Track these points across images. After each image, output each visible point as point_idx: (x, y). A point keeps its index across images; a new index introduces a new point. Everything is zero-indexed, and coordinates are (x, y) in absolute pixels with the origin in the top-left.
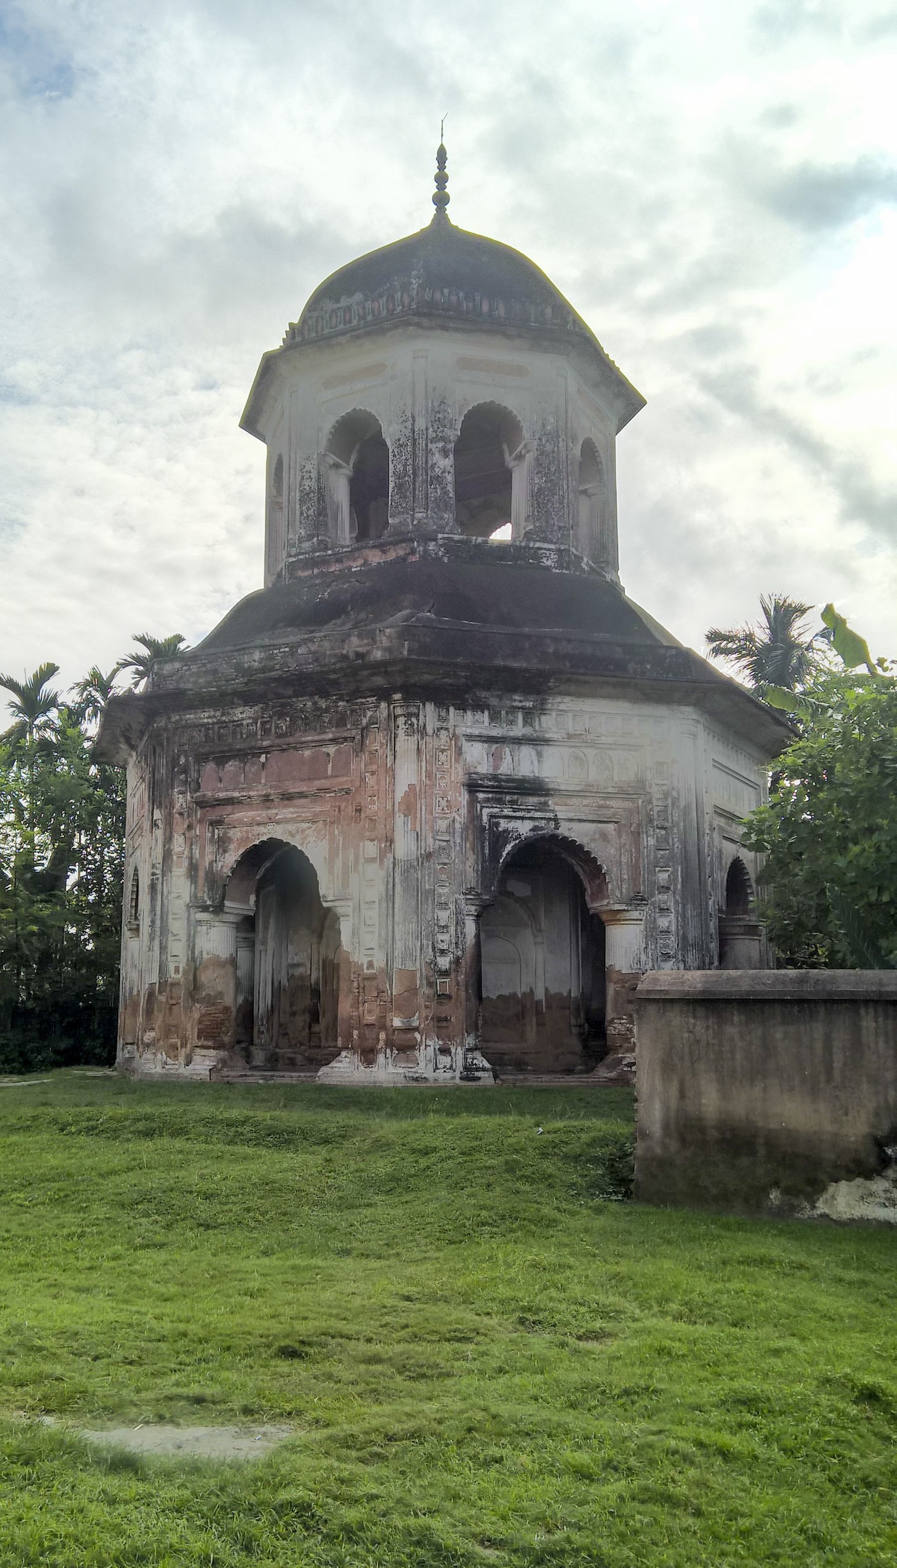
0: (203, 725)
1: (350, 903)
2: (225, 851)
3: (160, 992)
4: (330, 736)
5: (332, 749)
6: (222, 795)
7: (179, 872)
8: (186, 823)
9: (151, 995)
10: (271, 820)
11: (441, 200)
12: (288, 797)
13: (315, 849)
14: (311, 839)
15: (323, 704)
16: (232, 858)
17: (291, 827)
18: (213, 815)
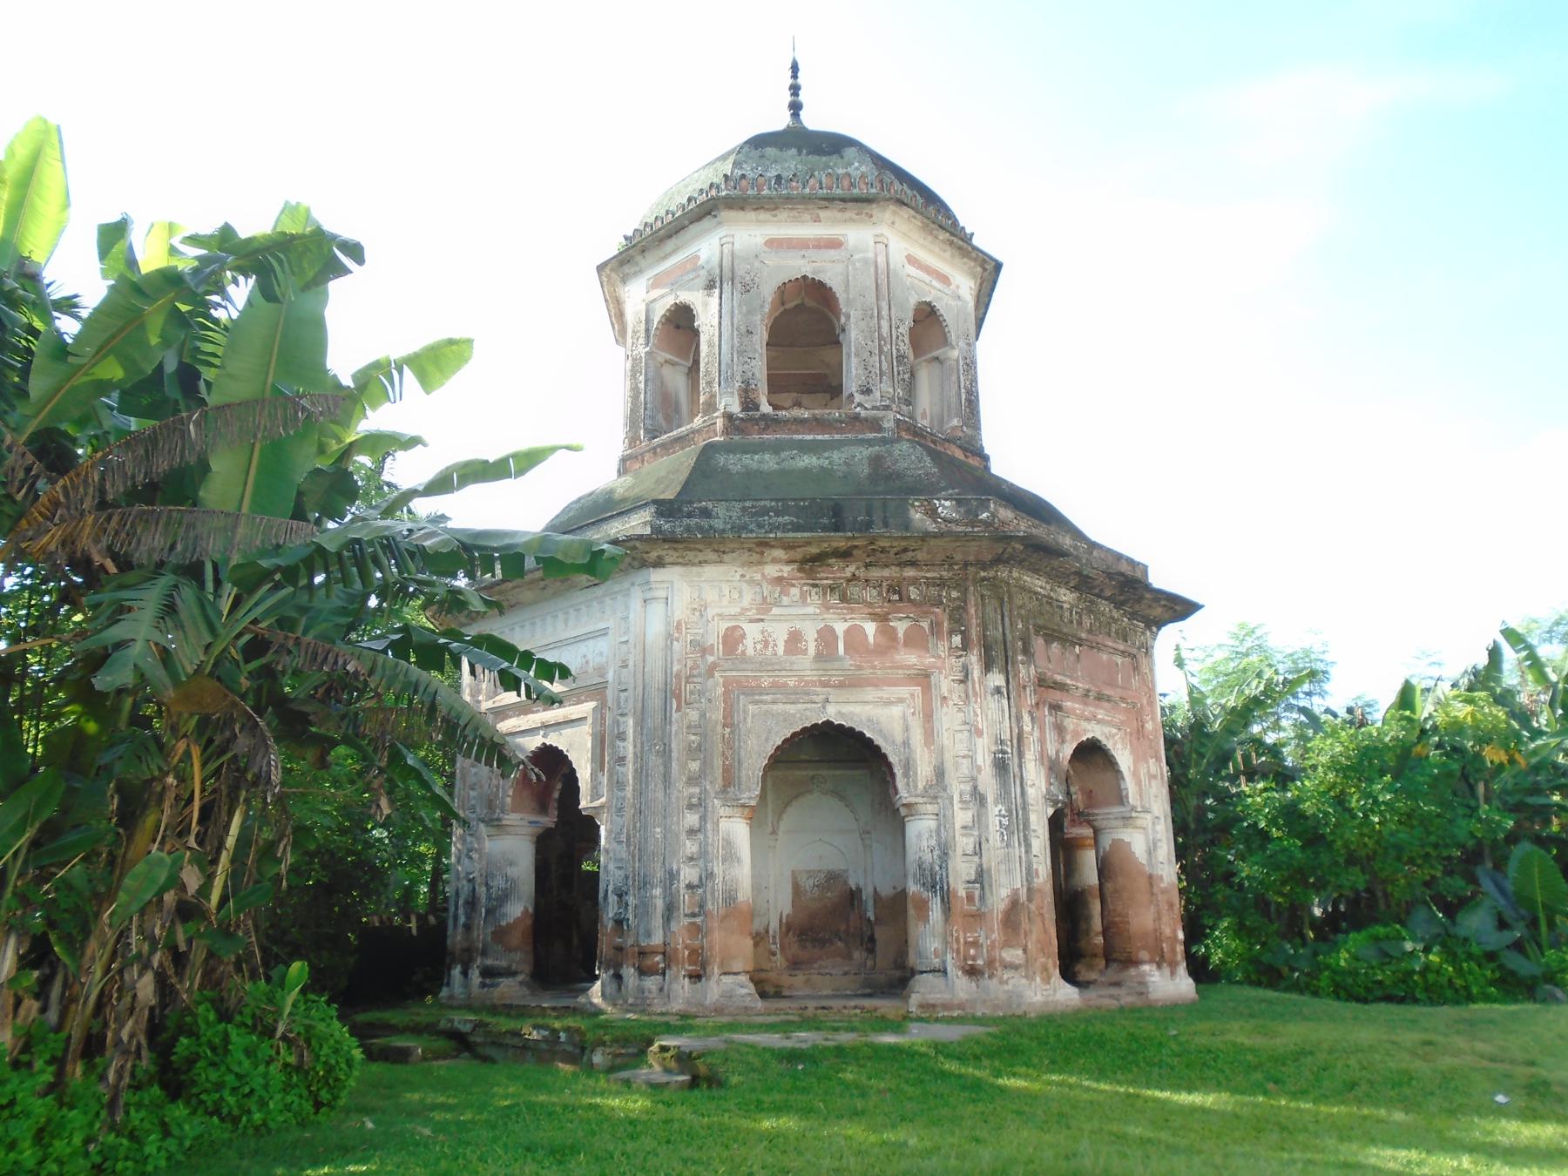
0: (1036, 593)
1: (1149, 816)
2: (1063, 742)
3: (1030, 899)
4: (1122, 648)
5: (1119, 660)
6: (1058, 678)
7: (1030, 755)
8: (1030, 699)
9: (1014, 904)
10: (1092, 718)
11: (796, 107)
12: (1100, 697)
13: (1124, 759)
14: (1119, 746)
15: (1116, 614)
16: (1068, 750)
17: (1106, 730)
18: (1055, 696)
